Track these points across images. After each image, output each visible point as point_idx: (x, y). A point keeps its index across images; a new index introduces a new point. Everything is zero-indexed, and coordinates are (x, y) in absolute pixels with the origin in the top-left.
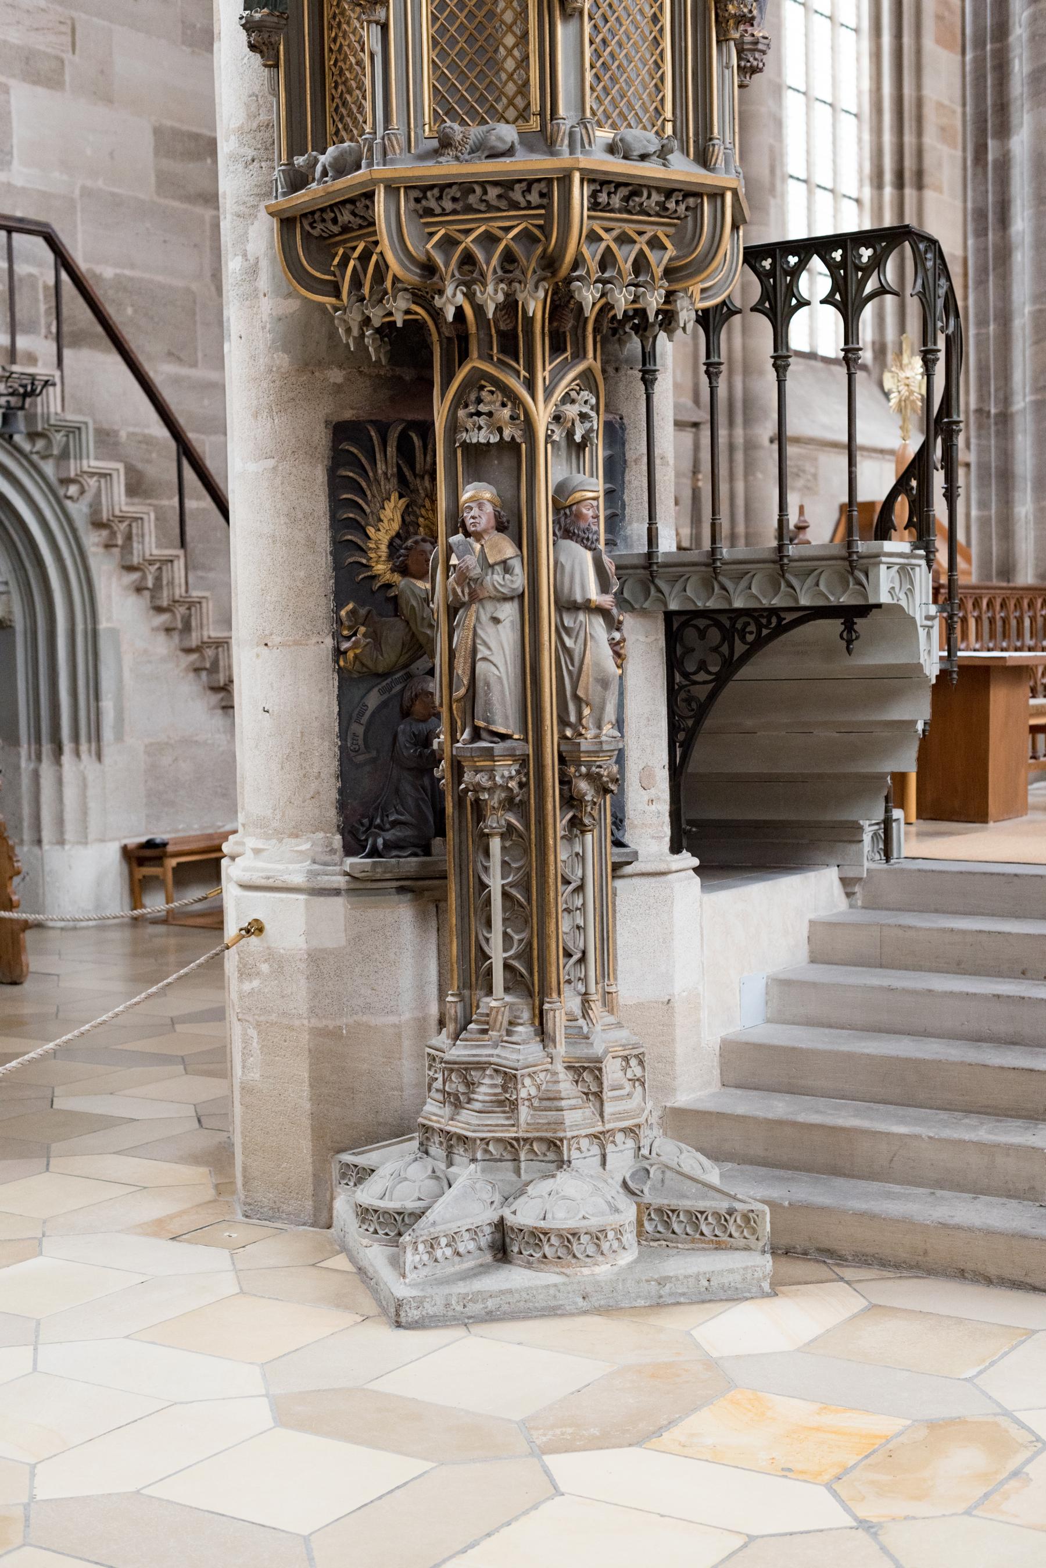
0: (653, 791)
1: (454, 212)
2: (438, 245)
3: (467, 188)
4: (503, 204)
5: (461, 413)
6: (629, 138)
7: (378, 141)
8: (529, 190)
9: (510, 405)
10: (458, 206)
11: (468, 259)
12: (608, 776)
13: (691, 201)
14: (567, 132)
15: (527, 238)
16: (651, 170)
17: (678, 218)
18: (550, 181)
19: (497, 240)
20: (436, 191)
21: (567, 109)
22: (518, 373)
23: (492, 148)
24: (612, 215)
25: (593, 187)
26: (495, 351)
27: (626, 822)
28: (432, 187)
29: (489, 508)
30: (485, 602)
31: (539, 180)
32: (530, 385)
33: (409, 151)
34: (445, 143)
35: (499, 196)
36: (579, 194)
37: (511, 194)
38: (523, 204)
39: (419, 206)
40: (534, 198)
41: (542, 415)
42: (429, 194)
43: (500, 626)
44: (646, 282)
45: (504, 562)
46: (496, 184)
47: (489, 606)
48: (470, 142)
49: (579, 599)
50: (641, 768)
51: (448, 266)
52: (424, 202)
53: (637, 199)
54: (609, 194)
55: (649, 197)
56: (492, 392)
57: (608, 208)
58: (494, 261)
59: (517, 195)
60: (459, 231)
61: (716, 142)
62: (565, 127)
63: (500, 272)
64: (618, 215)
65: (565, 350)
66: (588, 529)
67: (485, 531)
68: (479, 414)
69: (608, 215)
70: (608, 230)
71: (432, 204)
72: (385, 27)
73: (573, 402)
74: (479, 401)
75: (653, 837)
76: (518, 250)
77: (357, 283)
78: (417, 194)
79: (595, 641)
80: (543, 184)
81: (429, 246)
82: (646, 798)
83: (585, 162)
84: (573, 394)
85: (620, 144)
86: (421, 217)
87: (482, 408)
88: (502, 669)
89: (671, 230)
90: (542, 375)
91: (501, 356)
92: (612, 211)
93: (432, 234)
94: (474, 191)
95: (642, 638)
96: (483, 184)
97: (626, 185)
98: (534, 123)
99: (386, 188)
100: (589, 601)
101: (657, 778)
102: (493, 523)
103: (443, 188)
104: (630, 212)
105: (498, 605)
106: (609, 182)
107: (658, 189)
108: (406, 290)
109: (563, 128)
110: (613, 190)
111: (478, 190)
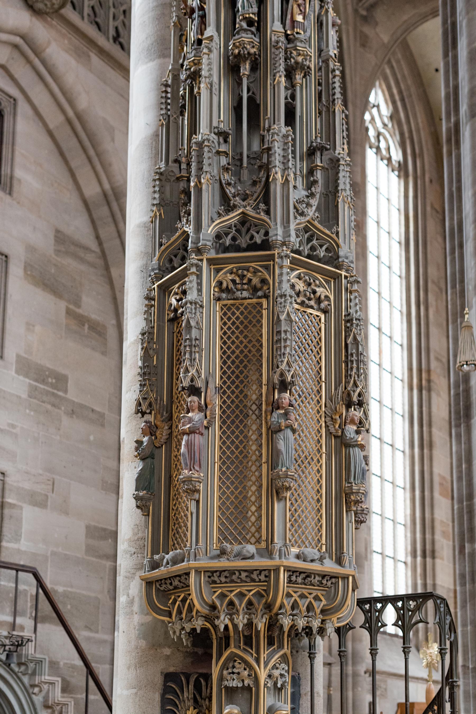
1: (226, 582)
2: (218, 597)
3: (232, 572)
4: (248, 580)
5: (225, 672)
6: (306, 552)
7: (193, 550)
8: (260, 574)
9: (248, 669)
10: (228, 580)
11: (231, 603)
15: (259, 595)
16: (316, 567)
18: (270, 571)
19: (244, 595)
20: (218, 573)
21: (278, 539)
22: (252, 655)
23: (244, 555)
24: (298, 586)
25: (289, 573)
28: (216, 571)
31: (265, 570)
32: (258, 660)
33: (206, 555)
34: (223, 552)
35: (247, 576)
36: (283, 576)
37: (252, 576)
38: (257, 580)
39: (210, 579)
40: (262, 577)
41: (263, 675)
42: (215, 574)
44: (312, 615)
46: (245, 571)
48: (234, 552)
51: (222, 607)
52: (212, 578)
53: (309, 579)
54: (296, 576)
55: (314, 578)
56: (240, 663)
57: (295, 582)
58: (243, 605)
59: (254, 576)
60: (227, 591)
62: (277, 547)
63: (245, 610)
64: (300, 586)
65: (274, 644)
68: (233, 673)
69: (296, 585)
70: (295, 592)
71: (216, 579)
73: (277, 668)
74: (234, 667)
76: (254, 600)
77: (180, 612)
78: (210, 574)
80: (267, 572)
81: (214, 597)
83: (286, 562)
86: (211, 584)
87: (235, 670)
90: (263, 656)
91: (244, 647)
92: (298, 584)
93: (215, 592)
94: (235, 574)
96: (239, 571)
97: (304, 573)
98: (263, 545)
99: (195, 571)
103: (221, 572)
104: (305, 584)
106: (297, 571)
107: (319, 575)
108: (202, 616)
109: (276, 547)
111: (237, 573)
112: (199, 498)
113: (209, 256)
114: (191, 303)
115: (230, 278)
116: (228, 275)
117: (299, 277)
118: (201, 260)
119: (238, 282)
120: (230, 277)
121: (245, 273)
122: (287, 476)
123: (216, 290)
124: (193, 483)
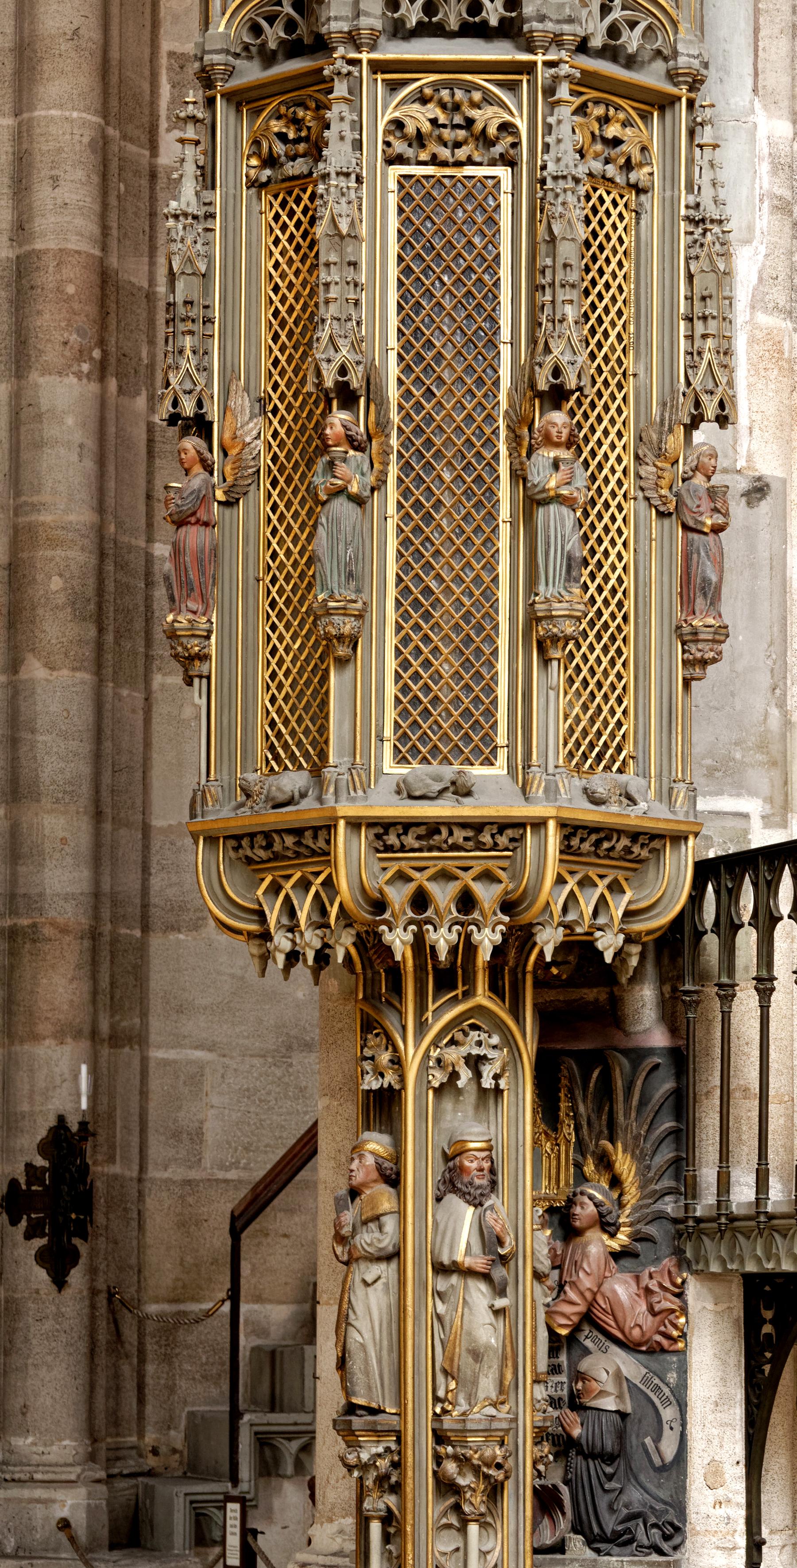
0: (720, 1492)
4: (302, 850)
12: (479, 1459)
13: (510, 832)
14: (333, 780)
17: (507, 849)
18: (328, 828)
21: (340, 755)
26: (384, 991)
27: (688, 1527)
29: (370, 1160)
30: (360, 1261)
40: (321, 843)
43: (370, 1290)
45: (377, 1218)
46: (290, 831)
47: (363, 1265)
49: (446, 1260)
50: (706, 1462)
53: (436, 837)
55: (451, 833)
59: (308, 840)
61: (533, 769)
66: (471, 1184)
67: (365, 1185)
70: (420, 869)
71: (249, 853)
72: (209, 678)
75: (718, 1548)
79: (470, 1309)
81: (260, 892)
82: (711, 1500)
83: (346, 809)
84: (459, 1036)
85: (402, 785)
88: (367, 1335)
89: (505, 863)
93: (263, 880)
95: (710, 1306)
96: (279, 832)
97: (418, 825)
100: (454, 1263)
101: (727, 1476)
102: (375, 1175)
104: (440, 850)
105: (370, 1265)
110: (401, 831)
112: (210, 672)
113: (235, 83)
114: (176, 217)
115: (276, 129)
116: (273, 123)
117: (424, 100)
118: (210, 102)
119: (291, 135)
120: (276, 126)
121: (301, 113)
122: (328, 612)
123: (254, 162)
124: (184, 640)
